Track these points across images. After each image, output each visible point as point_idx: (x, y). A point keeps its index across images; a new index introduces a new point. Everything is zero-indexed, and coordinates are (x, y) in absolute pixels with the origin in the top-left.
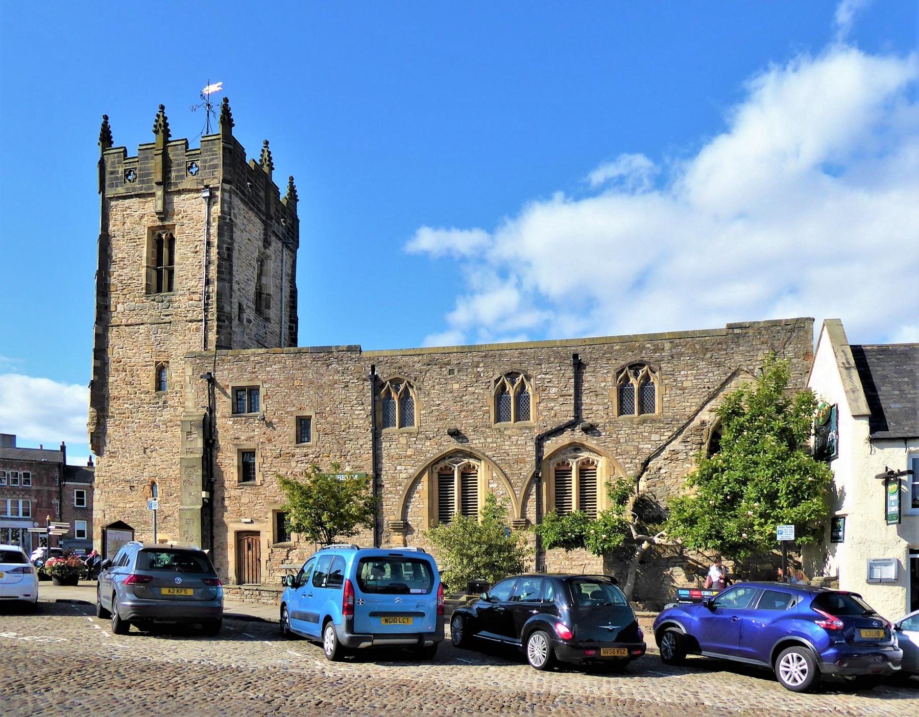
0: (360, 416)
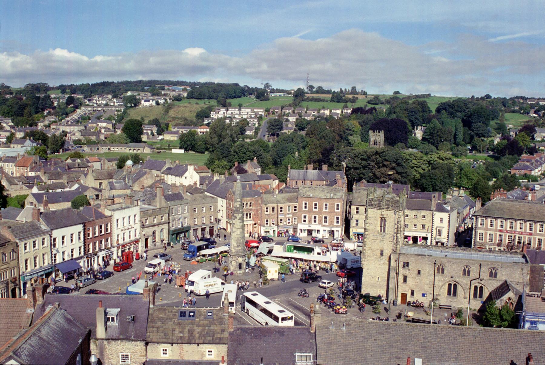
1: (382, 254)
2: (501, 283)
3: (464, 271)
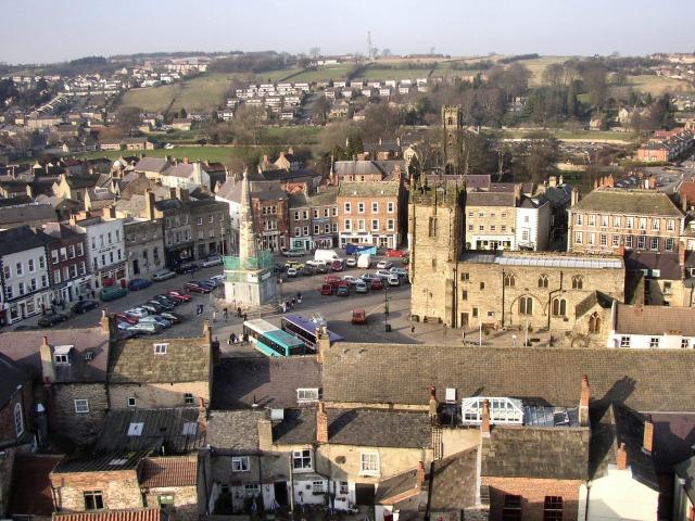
0: (499, 282)
1: (434, 264)
2: (589, 294)
3: (540, 282)
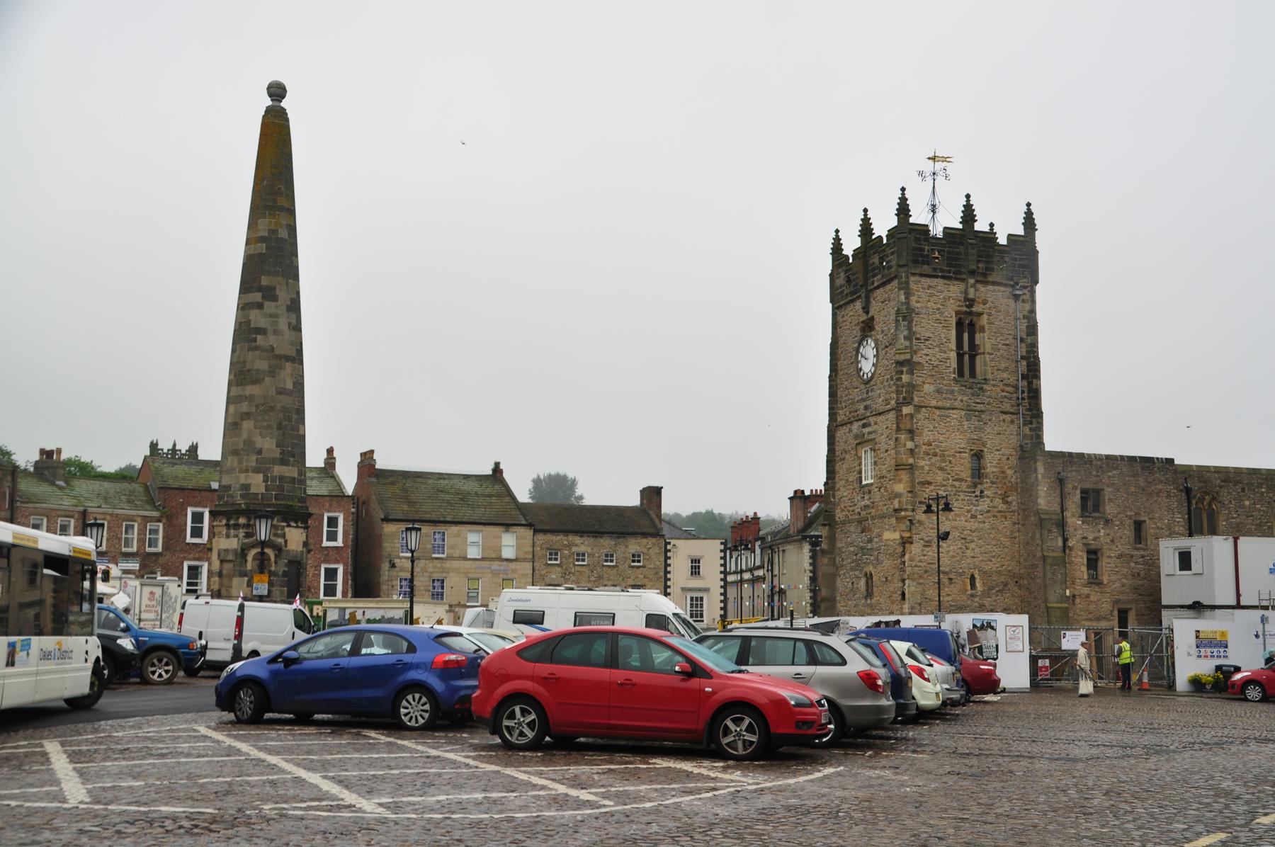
1: (978, 473)
